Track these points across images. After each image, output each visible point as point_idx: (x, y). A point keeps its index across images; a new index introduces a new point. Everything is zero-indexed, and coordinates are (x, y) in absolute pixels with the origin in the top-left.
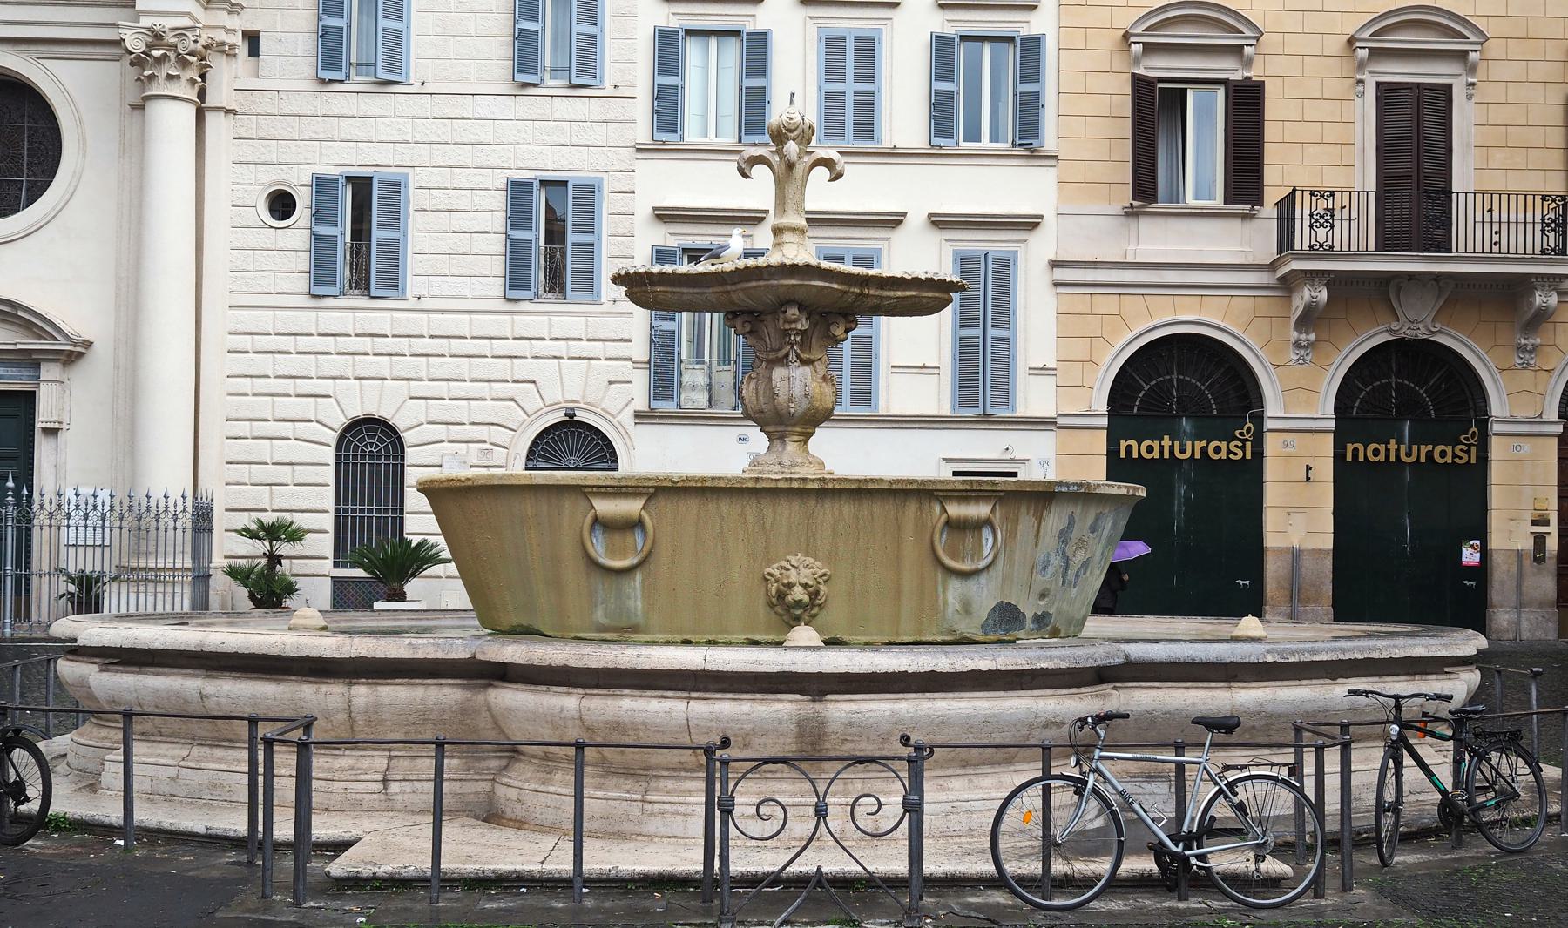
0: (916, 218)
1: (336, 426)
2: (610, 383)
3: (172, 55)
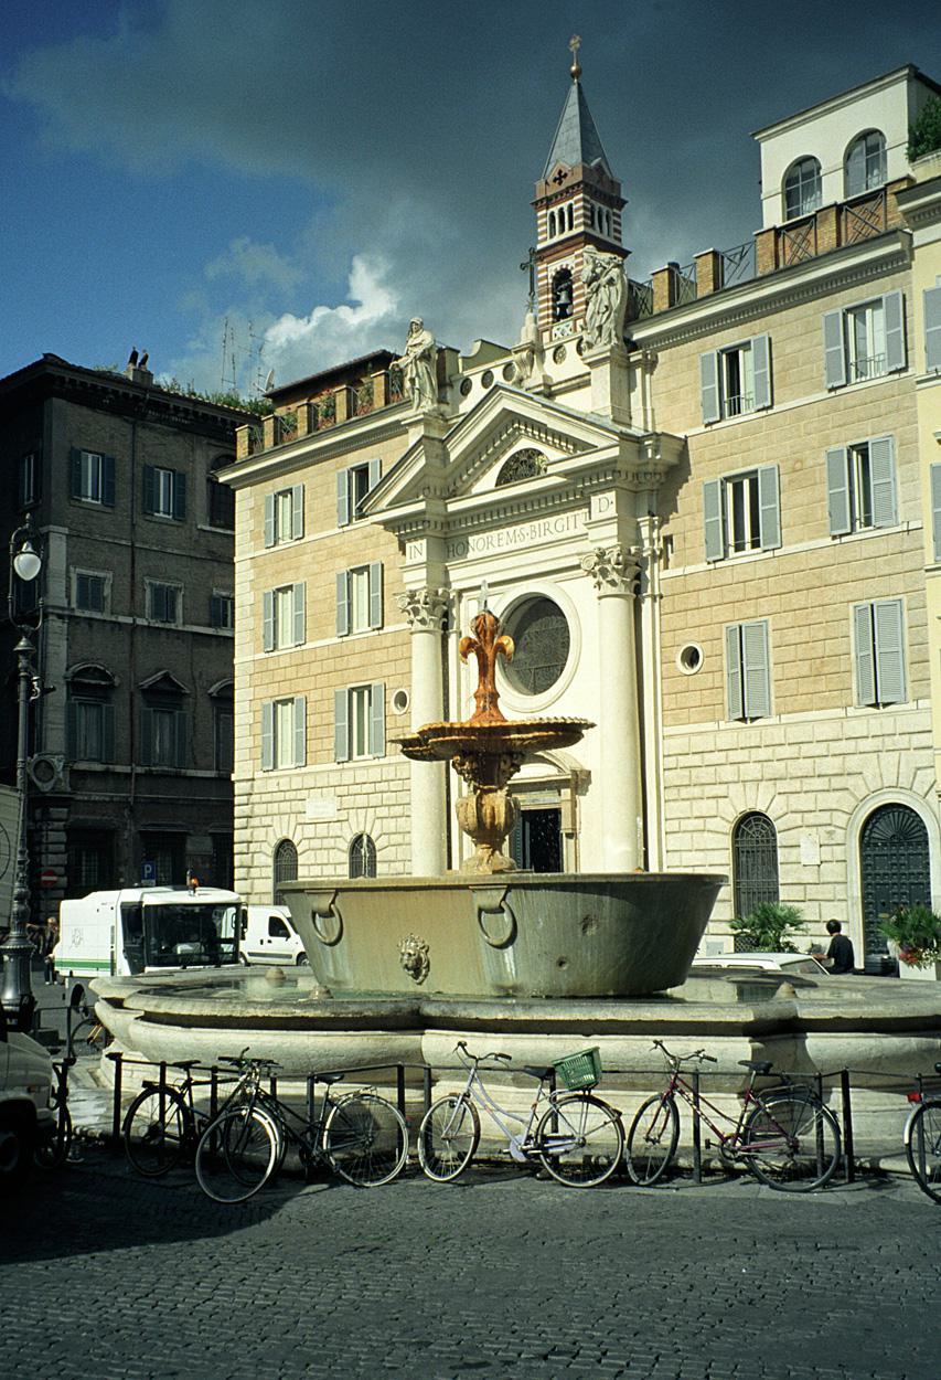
1: (731, 820)
2: (918, 769)
3: (609, 567)
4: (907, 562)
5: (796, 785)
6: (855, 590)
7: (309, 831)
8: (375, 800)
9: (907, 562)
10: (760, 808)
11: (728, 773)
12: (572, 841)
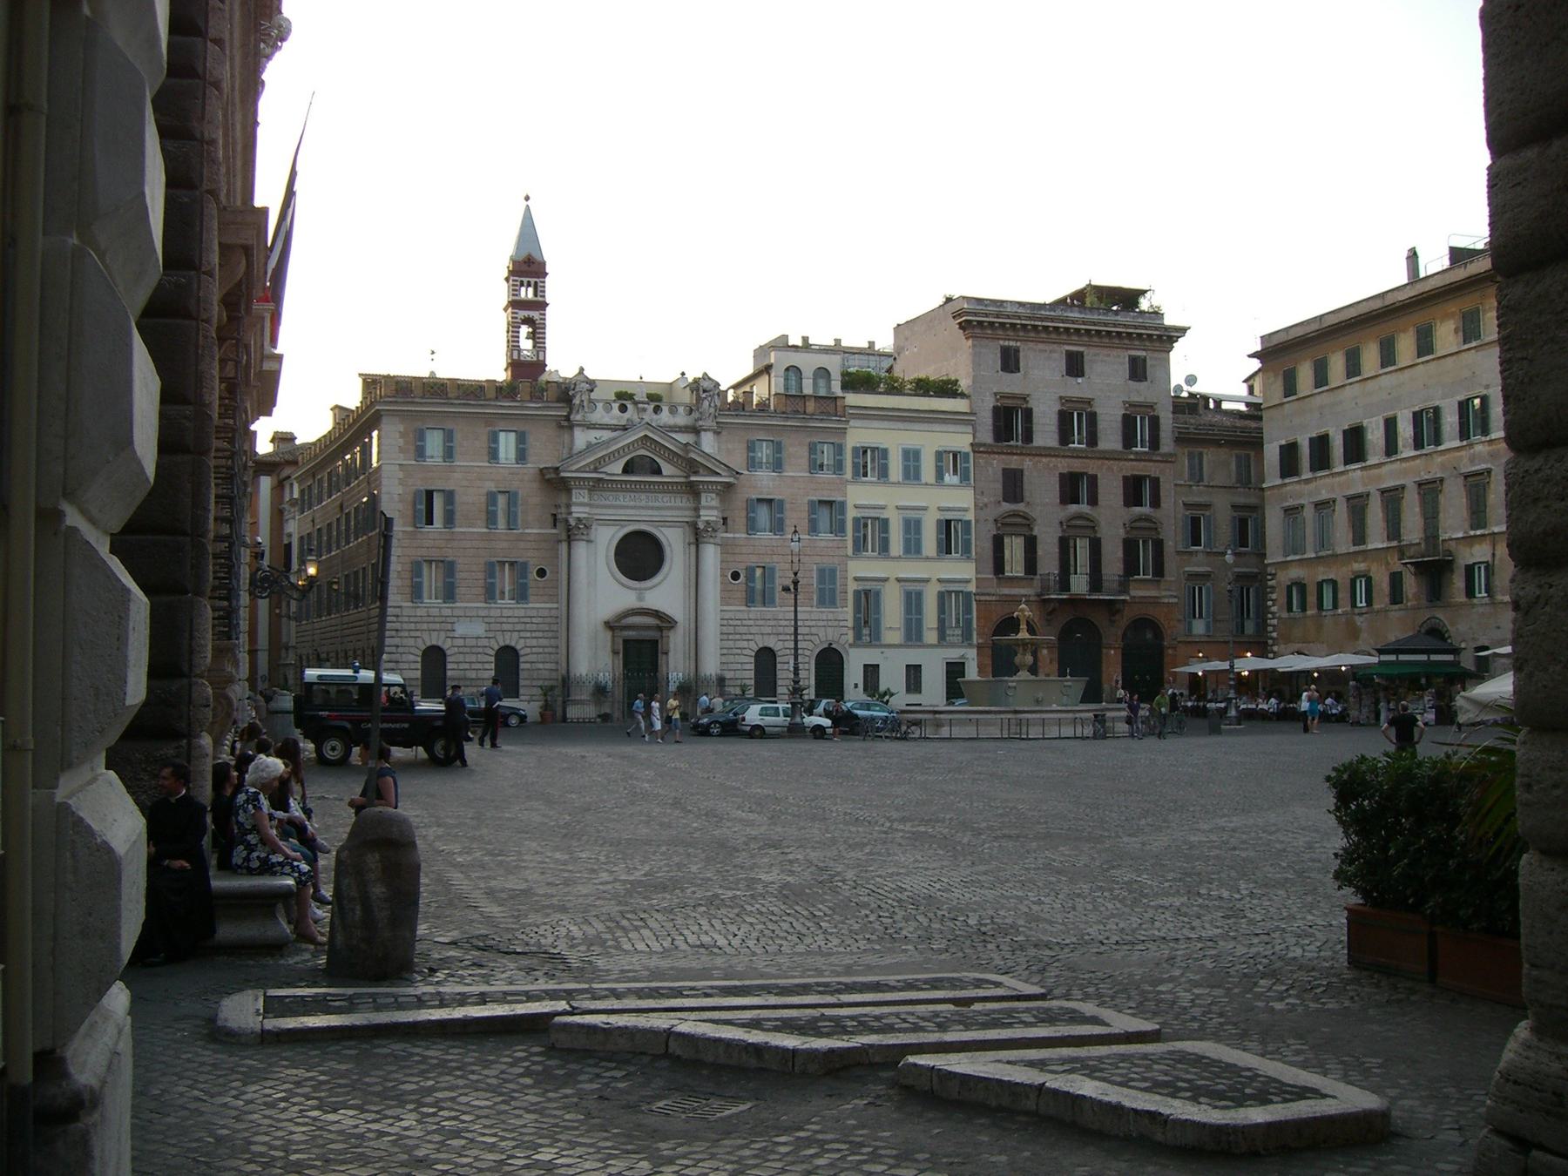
0: (934, 580)
6: (818, 559)
7: (460, 642)
8: (519, 627)
10: (771, 646)
11: (753, 630)
12: (664, 656)
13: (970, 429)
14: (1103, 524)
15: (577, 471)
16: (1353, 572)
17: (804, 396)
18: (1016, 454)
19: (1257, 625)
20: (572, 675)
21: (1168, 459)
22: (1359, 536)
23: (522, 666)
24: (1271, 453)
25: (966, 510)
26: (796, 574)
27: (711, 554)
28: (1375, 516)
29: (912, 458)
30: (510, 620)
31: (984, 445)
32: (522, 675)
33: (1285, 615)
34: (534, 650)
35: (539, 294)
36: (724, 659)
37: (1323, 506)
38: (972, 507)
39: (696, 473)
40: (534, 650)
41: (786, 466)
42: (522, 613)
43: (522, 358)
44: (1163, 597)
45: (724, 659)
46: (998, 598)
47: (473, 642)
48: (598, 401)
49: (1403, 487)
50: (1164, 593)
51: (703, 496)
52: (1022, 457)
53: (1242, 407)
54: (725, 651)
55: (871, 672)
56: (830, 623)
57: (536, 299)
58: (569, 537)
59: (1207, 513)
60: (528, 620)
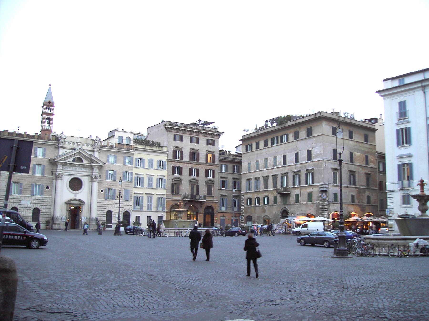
4: (131, 186)
5: (116, 208)
7: (23, 206)
8: (40, 202)
9: (131, 186)
11: (106, 206)
13: (166, 155)
14: (200, 182)
15: (59, 160)
16: (264, 196)
17: (123, 144)
18: (178, 162)
19: (238, 209)
20: (55, 216)
21: (217, 165)
22: (266, 186)
23: (40, 213)
24: (244, 165)
25: (165, 176)
26: (120, 190)
27: (95, 185)
28: (270, 181)
29: (151, 162)
30: (38, 200)
31: (170, 160)
32: (40, 216)
33: (246, 206)
34: (44, 209)
35: (52, 111)
36: (98, 213)
37: (257, 179)
38: (166, 175)
39: (93, 163)
40: (44, 209)
41: (117, 162)
42: (41, 199)
43: (46, 129)
44: (215, 201)
45: (98, 213)
46: (172, 200)
47: (26, 206)
48: (67, 141)
49: (278, 175)
50: (215, 200)
51: (94, 169)
52: (180, 163)
53: (235, 153)
54: (98, 211)
55: (138, 218)
56: (127, 205)
57: (51, 113)
58: (56, 178)
59: (226, 180)
60: (43, 201)
